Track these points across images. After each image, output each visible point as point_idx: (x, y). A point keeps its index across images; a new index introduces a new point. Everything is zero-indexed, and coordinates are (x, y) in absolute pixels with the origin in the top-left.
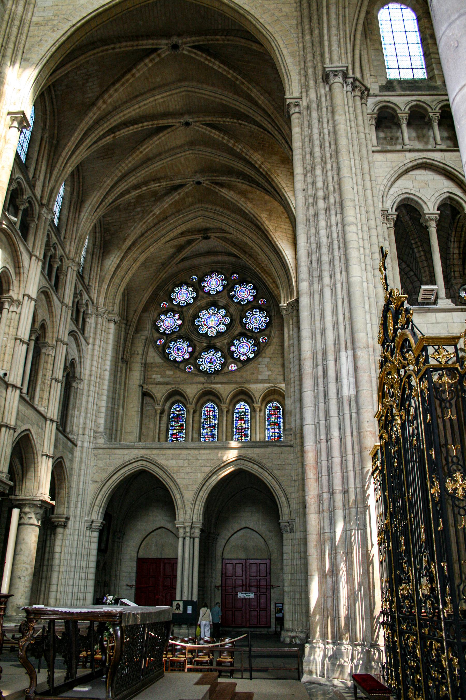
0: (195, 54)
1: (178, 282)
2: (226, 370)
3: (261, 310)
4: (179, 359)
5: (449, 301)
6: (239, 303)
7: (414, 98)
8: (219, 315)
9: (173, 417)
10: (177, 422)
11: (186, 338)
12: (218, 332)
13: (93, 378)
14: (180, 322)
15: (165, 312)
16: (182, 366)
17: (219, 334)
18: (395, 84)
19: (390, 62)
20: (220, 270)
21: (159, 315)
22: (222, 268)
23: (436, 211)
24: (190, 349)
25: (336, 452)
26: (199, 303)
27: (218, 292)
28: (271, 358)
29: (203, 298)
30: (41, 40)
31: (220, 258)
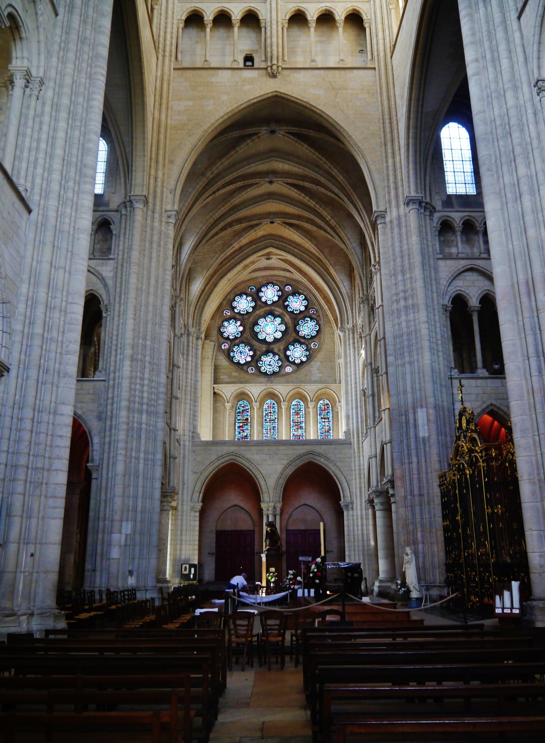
0: (288, 137)
1: (238, 292)
2: (283, 372)
3: (312, 319)
4: (242, 362)
5: (484, 371)
6: (292, 312)
7: (466, 214)
8: (275, 323)
9: (239, 413)
10: (243, 417)
11: (247, 344)
12: (275, 338)
13: (189, 388)
14: (241, 329)
15: (228, 320)
16: (245, 367)
17: (276, 340)
18: (453, 198)
19: (449, 177)
20: (275, 282)
21: (223, 322)
22: (277, 281)
23: (478, 305)
24: (251, 353)
25: (415, 471)
26: (258, 312)
27: (274, 303)
28: (321, 362)
29: (261, 307)
30: (181, 144)
31: (276, 272)
